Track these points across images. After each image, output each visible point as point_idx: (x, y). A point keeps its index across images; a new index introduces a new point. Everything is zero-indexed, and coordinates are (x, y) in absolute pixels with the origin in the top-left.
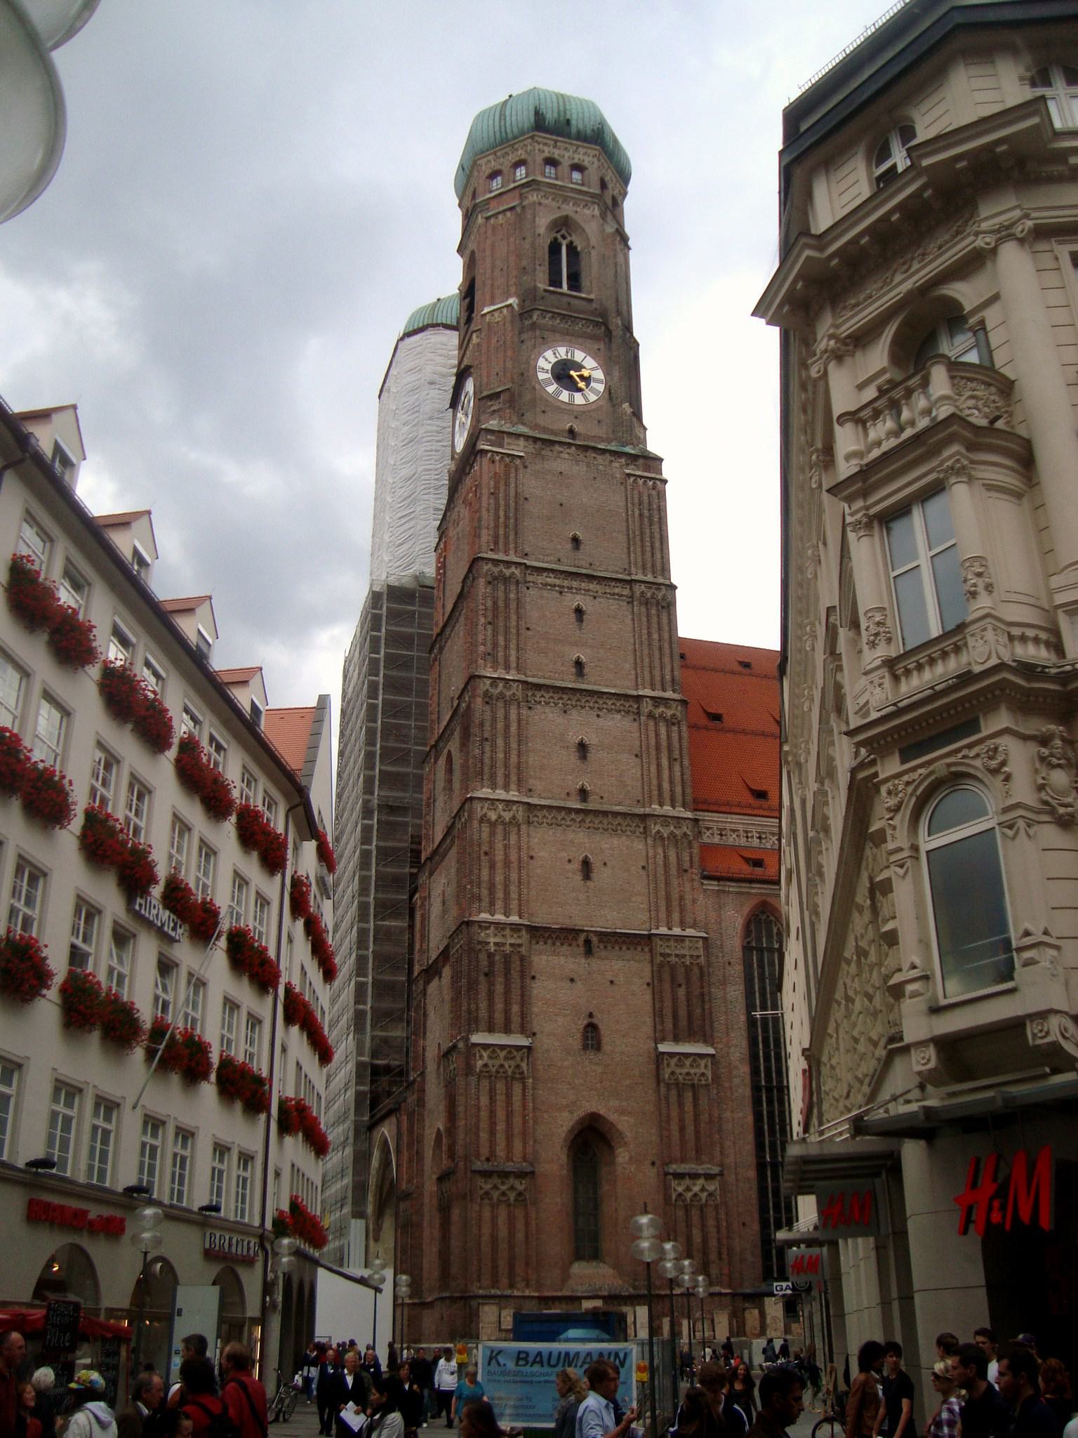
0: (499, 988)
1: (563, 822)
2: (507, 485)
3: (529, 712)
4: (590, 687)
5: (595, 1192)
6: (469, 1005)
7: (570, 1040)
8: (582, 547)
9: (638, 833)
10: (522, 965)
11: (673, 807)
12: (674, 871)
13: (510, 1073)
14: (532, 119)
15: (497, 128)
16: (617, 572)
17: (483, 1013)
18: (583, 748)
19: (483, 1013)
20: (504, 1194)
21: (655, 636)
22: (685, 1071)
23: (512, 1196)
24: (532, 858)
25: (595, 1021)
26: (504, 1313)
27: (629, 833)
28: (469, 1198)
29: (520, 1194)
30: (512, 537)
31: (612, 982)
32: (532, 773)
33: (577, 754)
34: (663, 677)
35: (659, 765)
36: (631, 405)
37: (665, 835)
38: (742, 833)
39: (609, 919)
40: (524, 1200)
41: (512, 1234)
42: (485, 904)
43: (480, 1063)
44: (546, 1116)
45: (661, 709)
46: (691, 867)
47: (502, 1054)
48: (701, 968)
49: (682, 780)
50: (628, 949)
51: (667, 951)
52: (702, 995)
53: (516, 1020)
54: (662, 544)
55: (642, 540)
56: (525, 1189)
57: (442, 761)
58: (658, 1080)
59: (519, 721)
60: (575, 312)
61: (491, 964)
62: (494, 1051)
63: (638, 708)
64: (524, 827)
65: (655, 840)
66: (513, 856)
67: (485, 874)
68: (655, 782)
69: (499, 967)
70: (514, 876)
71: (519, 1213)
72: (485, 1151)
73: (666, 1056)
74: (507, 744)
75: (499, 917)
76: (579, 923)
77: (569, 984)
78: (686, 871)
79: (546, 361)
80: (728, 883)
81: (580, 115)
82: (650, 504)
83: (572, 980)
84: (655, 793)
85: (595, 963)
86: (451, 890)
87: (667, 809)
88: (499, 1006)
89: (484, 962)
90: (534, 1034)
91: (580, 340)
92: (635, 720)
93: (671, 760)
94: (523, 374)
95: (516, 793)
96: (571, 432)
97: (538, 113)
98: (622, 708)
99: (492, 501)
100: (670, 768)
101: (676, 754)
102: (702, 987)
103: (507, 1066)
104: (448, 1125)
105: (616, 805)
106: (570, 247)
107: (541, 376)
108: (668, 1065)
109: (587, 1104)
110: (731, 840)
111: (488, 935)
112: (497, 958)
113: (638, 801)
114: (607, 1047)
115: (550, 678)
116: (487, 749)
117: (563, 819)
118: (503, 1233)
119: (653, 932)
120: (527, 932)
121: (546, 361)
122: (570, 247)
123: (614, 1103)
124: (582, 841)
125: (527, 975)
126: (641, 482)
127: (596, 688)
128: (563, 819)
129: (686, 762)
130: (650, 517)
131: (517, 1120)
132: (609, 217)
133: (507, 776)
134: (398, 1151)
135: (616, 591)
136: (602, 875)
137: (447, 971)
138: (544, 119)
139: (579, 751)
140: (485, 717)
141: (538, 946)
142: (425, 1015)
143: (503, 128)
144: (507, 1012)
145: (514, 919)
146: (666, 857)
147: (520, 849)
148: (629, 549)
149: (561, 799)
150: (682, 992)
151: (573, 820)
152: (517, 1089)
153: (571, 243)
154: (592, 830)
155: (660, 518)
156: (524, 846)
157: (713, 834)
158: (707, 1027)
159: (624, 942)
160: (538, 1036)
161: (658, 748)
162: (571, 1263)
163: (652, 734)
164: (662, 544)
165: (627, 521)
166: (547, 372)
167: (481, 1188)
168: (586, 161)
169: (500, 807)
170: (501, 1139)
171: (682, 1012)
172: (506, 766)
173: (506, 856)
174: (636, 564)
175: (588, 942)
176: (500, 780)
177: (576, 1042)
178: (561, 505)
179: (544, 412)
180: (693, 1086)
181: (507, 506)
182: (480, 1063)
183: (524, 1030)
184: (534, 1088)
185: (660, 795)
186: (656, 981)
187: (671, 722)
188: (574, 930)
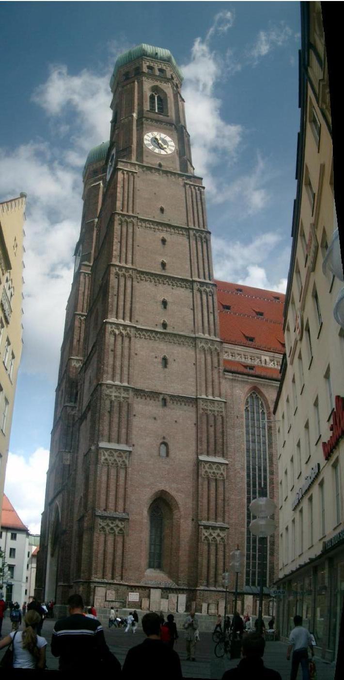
0: (116, 420)
3: (137, 284)
4: (169, 275)
5: (161, 532)
9: (191, 346)
10: (128, 408)
11: (209, 334)
12: (209, 367)
13: (119, 465)
17: (106, 432)
18: (165, 303)
19: (106, 432)
20: (112, 529)
22: (212, 471)
23: (117, 530)
24: (136, 354)
25: (165, 441)
26: (108, 592)
27: (187, 346)
29: (121, 530)
31: (176, 421)
37: (206, 348)
38: (243, 356)
39: (176, 389)
40: (123, 533)
41: (115, 550)
42: (110, 376)
43: (103, 458)
44: (137, 489)
45: (205, 287)
47: (116, 454)
48: (222, 418)
50: (185, 405)
51: (205, 407)
52: (223, 432)
53: (123, 437)
56: (124, 527)
61: (112, 406)
62: (111, 452)
64: (133, 339)
65: (200, 351)
66: (126, 353)
69: (116, 409)
70: (126, 363)
71: (119, 539)
72: (103, 505)
73: (203, 462)
75: (117, 383)
76: (160, 389)
77: (153, 420)
78: (216, 368)
80: (237, 375)
83: (155, 419)
85: (167, 411)
87: (207, 336)
88: (115, 428)
90: (133, 445)
95: (129, 322)
101: (211, 310)
102: (223, 428)
103: (118, 460)
108: (204, 467)
109: (160, 485)
110: (238, 359)
111: (111, 392)
114: (172, 454)
118: (110, 550)
119: (198, 397)
120: (132, 391)
123: (174, 485)
124: (163, 348)
127: (172, 275)
131: (121, 491)
136: (173, 366)
141: (137, 400)
144: (119, 432)
145: (126, 384)
146: (206, 359)
147: (130, 349)
149: (153, 327)
150: (212, 429)
151: (158, 338)
152: (122, 474)
154: (168, 343)
156: (132, 348)
157: (228, 355)
158: (225, 449)
159: (183, 401)
160: (135, 447)
162: (146, 570)
167: (100, 525)
170: (112, 498)
171: (212, 440)
173: (122, 352)
175: (164, 400)
176: (121, 314)
182: (103, 458)
183: (127, 442)
188: (157, 393)
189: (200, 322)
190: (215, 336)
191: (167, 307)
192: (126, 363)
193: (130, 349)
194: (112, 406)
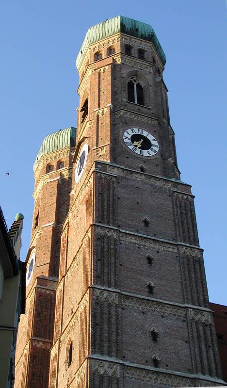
1: (144, 378)
2: (109, 190)
8: (150, 225)
14: (119, 27)
15: (101, 32)
16: (169, 240)
18: (154, 336)
21: (193, 276)
30: (111, 216)
32: (125, 347)
33: (152, 338)
34: (199, 299)
35: (200, 349)
36: (172, 159)
49: (215, 359)
54: (193, 228)
55: (183, 225)
59: (117, 315)
60: (142, 113)
63: (185, 314)
68: (198, 359)
74: (110, 328)
79: (128, 134)
81: (143, 28)
82: (186, 207)
84: (199, 366)
93: (208, 347)
94: (115, 140)
96: (142, 169)
97: (122, 24)
98: (176, 314)
99: (100, 198)
100: (207, 351)
105: (176, 371)
106: (139, 86)
107: (126, 140)
113: (189, 370)
115: (134, 293)
116: (98, 331)
117: (144, 377)
121: (128, 134)
122: (139, 86)
126: (180, 196)
128: (144, 377)
129: (216, 349)
130: (186, 214)
132: (157, 75)
133: (110, 347)
135: (170, 250)
138: (125, 28)
139: (152, 336)
140: (97, 312)
143: (104, 32)
148: (175, 228)
149: (142, 364)
153: (139, 83)
155: (191, 215)
163: (195, 330)
164: (193, 228)
165: (174, 215)
166: (129, 139)
168: (146, 48)
169: (106, 365)
174: (180, 236)
176: (106, 349)
179: (127, 157)
181: (108, 200)
185: (202, 367)
187: (205, 325)
190: (217, 376)
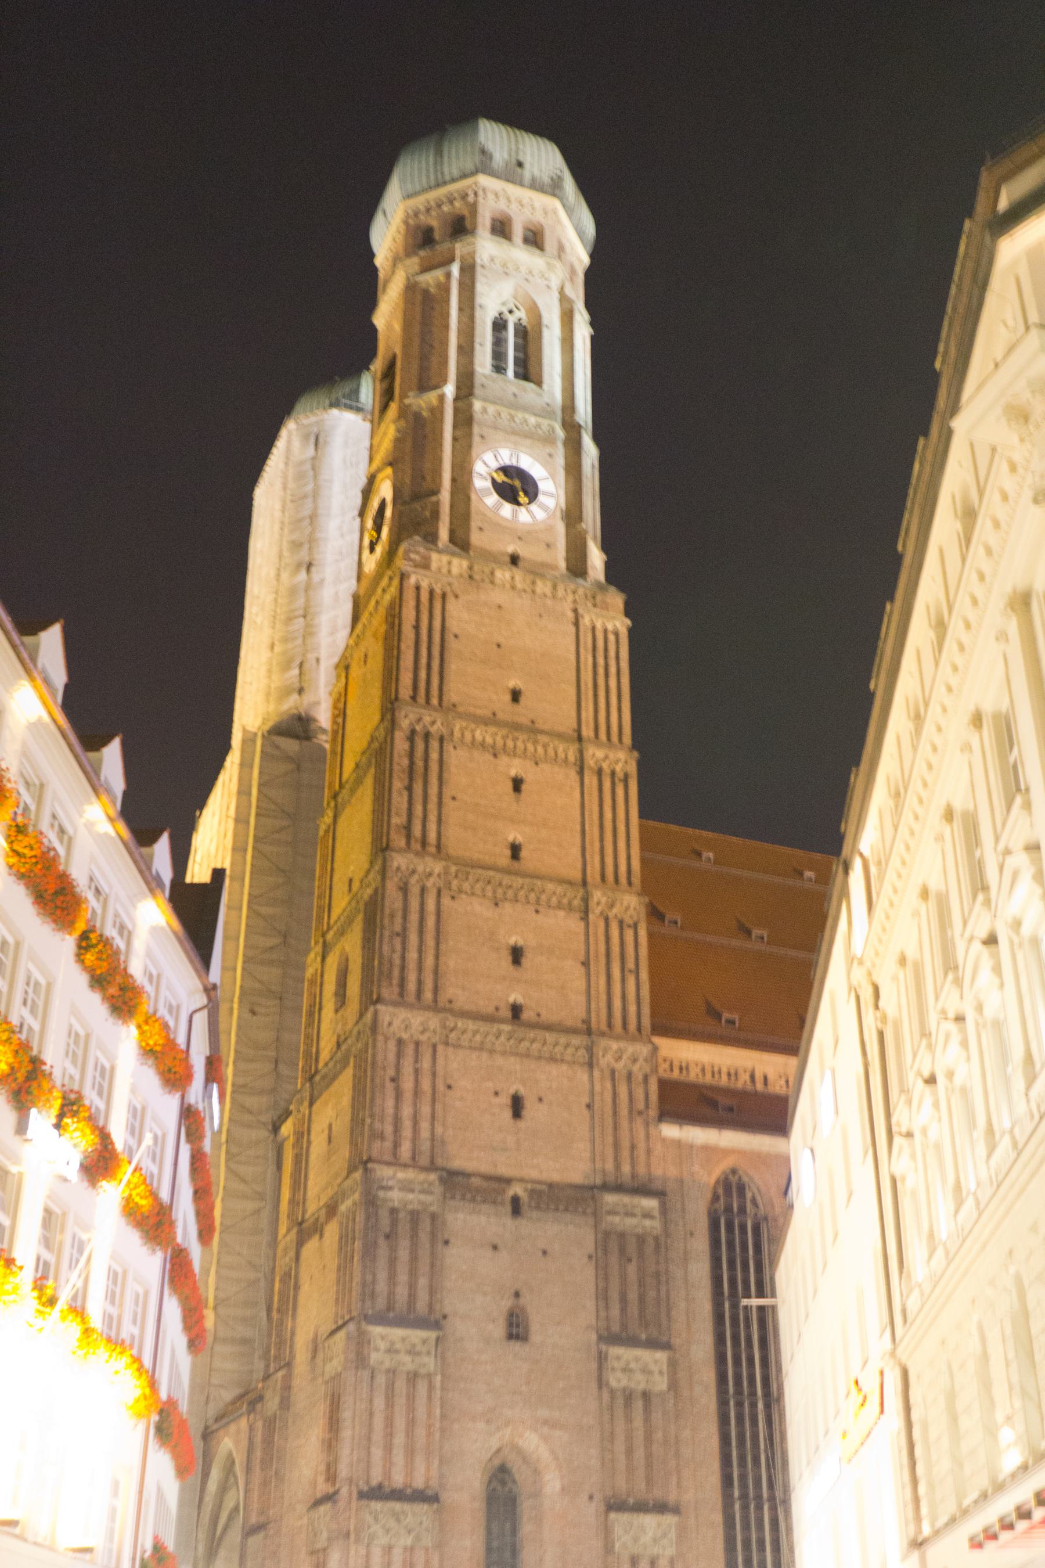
0: (403, 1253)
5: (514, 1532)
6: (364, 1274)
7: (491, 1327)
12: (624, 1111)
24: (449, 1087)
28: (352, 1537)
31: (545, 1253)
46: (647, 1106)
52: (657, 1274)
57: (333, 961)
58: (601, 1383)
61: (394, 1222)
66: (426, 1084)
67: (390, 1103)
70: (425, 1110)
77: (490, 1253)
83: (495, 1247)
86: (342, 1126)
88: (403, 1277)
89: (385, 1222)
91: (528, 442)
92: (582, 919)
100: (623, 980)
101: (631, 964)
102: (658, 1263)
104: (327, 1436)
112: (402, 1215)
114: (536, 1337)
125: (440, 1239)
129: (644, 975)
134: (248, 1469)
137: (332, 1230)
141: (452, 1203)
142: (297, 1287)
147: (434, 1074)
150: (632, 1269)
158: (663, 1316)
161: (608, 955)
171: (633, 1296)
172: (420, 969)
175: (516, 1202)
177: (499, 1330)
178: (499, 646)
180: (646, 1396)
184: (443, 1389)
186: (600, 1254)
189: (603, 997)
191: (524, 961)
192: (425, 1110)
193: (434, 1074)
194: (394, 1222)
